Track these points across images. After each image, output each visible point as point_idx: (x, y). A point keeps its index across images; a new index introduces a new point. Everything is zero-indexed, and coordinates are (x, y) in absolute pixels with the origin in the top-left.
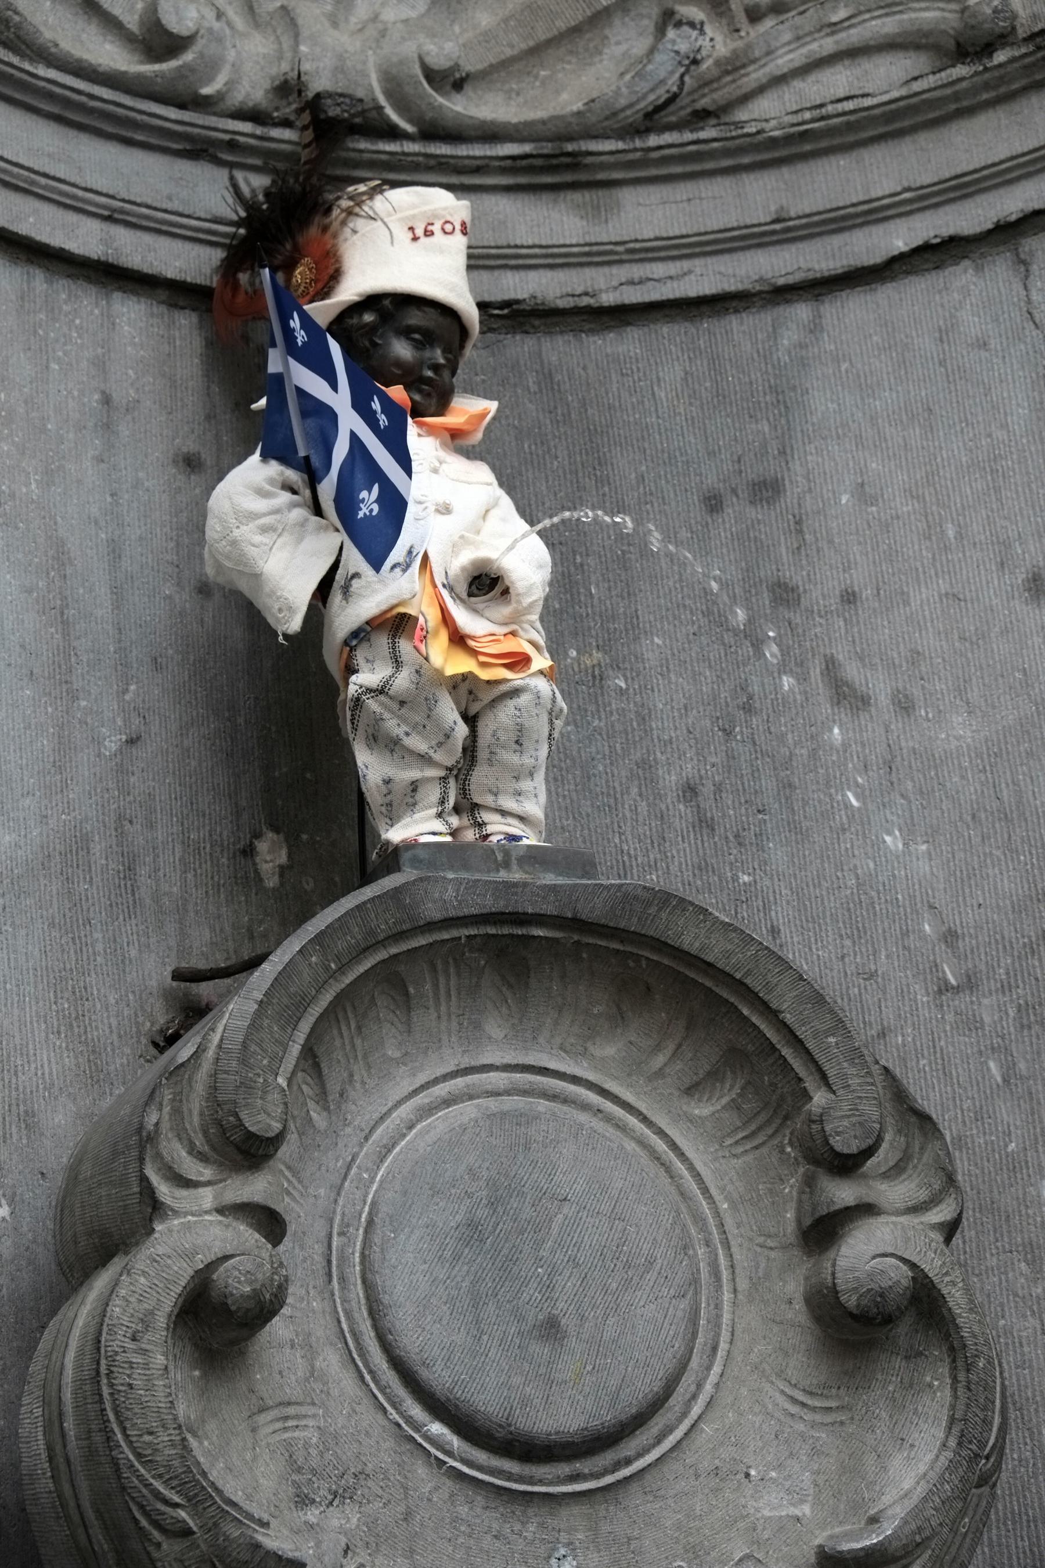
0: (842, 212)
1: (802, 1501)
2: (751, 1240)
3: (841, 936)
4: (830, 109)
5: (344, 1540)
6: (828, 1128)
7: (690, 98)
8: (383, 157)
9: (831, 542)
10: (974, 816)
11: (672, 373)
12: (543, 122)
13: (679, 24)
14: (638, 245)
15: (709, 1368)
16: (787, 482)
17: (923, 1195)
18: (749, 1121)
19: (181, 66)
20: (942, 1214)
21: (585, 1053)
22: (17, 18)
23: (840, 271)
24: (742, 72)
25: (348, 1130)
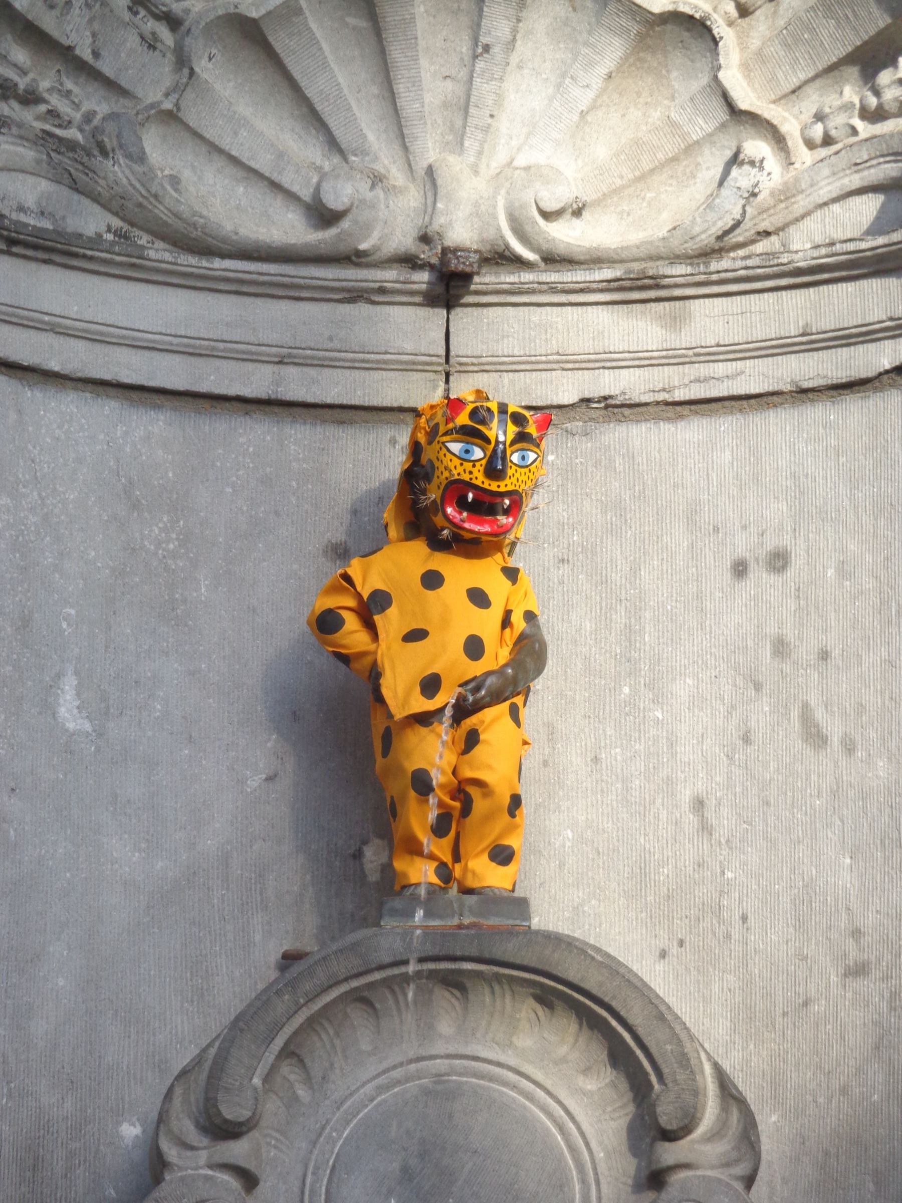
0: (847, 332)
2: (616, 1179)
3: (788, 924)
4: (838, 248)
7: (753, 222)
16: (793, 555)
17: (734, 1155)
19: (340, 233)
22: (202, 221)
23: (844, 381)
24: (793, 200)
25: (327, 1102)
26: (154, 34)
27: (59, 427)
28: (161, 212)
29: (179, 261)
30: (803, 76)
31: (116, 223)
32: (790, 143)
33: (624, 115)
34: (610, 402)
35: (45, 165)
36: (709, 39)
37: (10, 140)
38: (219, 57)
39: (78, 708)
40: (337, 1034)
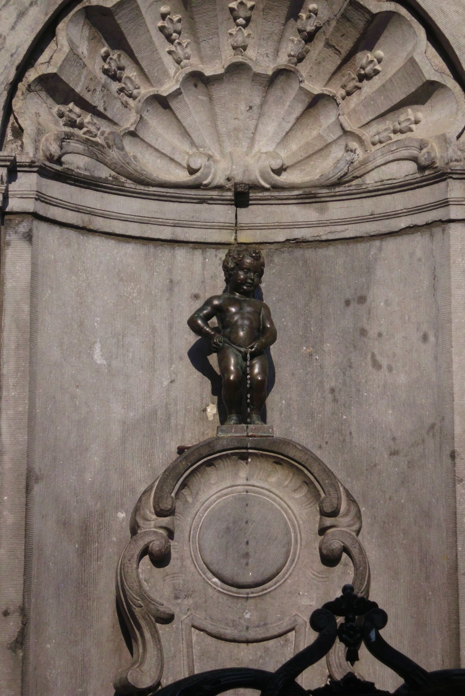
0: (388, 214)
1: (313, 601)
2: (307, 532)
5: (188, 607)
6: (324, 505)
8: (258, 197)
9: (377, 317)
10: (403, 405)
11: (340, 261)
12: (308, 182)
13: (347, 151)
14: (333, 221)
15: (291, 566)
17: (352, 522)
18: (308, 501)
20: (355, 527)
21: (266, 480)
22: (145, 172)
24: (367, 164)
25: (198, 503)
26: (126, 101)
27: (93, 250)
28: (130, 169)
29: (137, 188)
30: (371, 118)
31: (113, 173)
32: (366, 143)
33: (302, 133)
34: (297, 240)
35: (87, 151)
36: (335, 104)
37: (74, 141)
38: (151, 110)
39: (101, 355)
40: (202, 477)
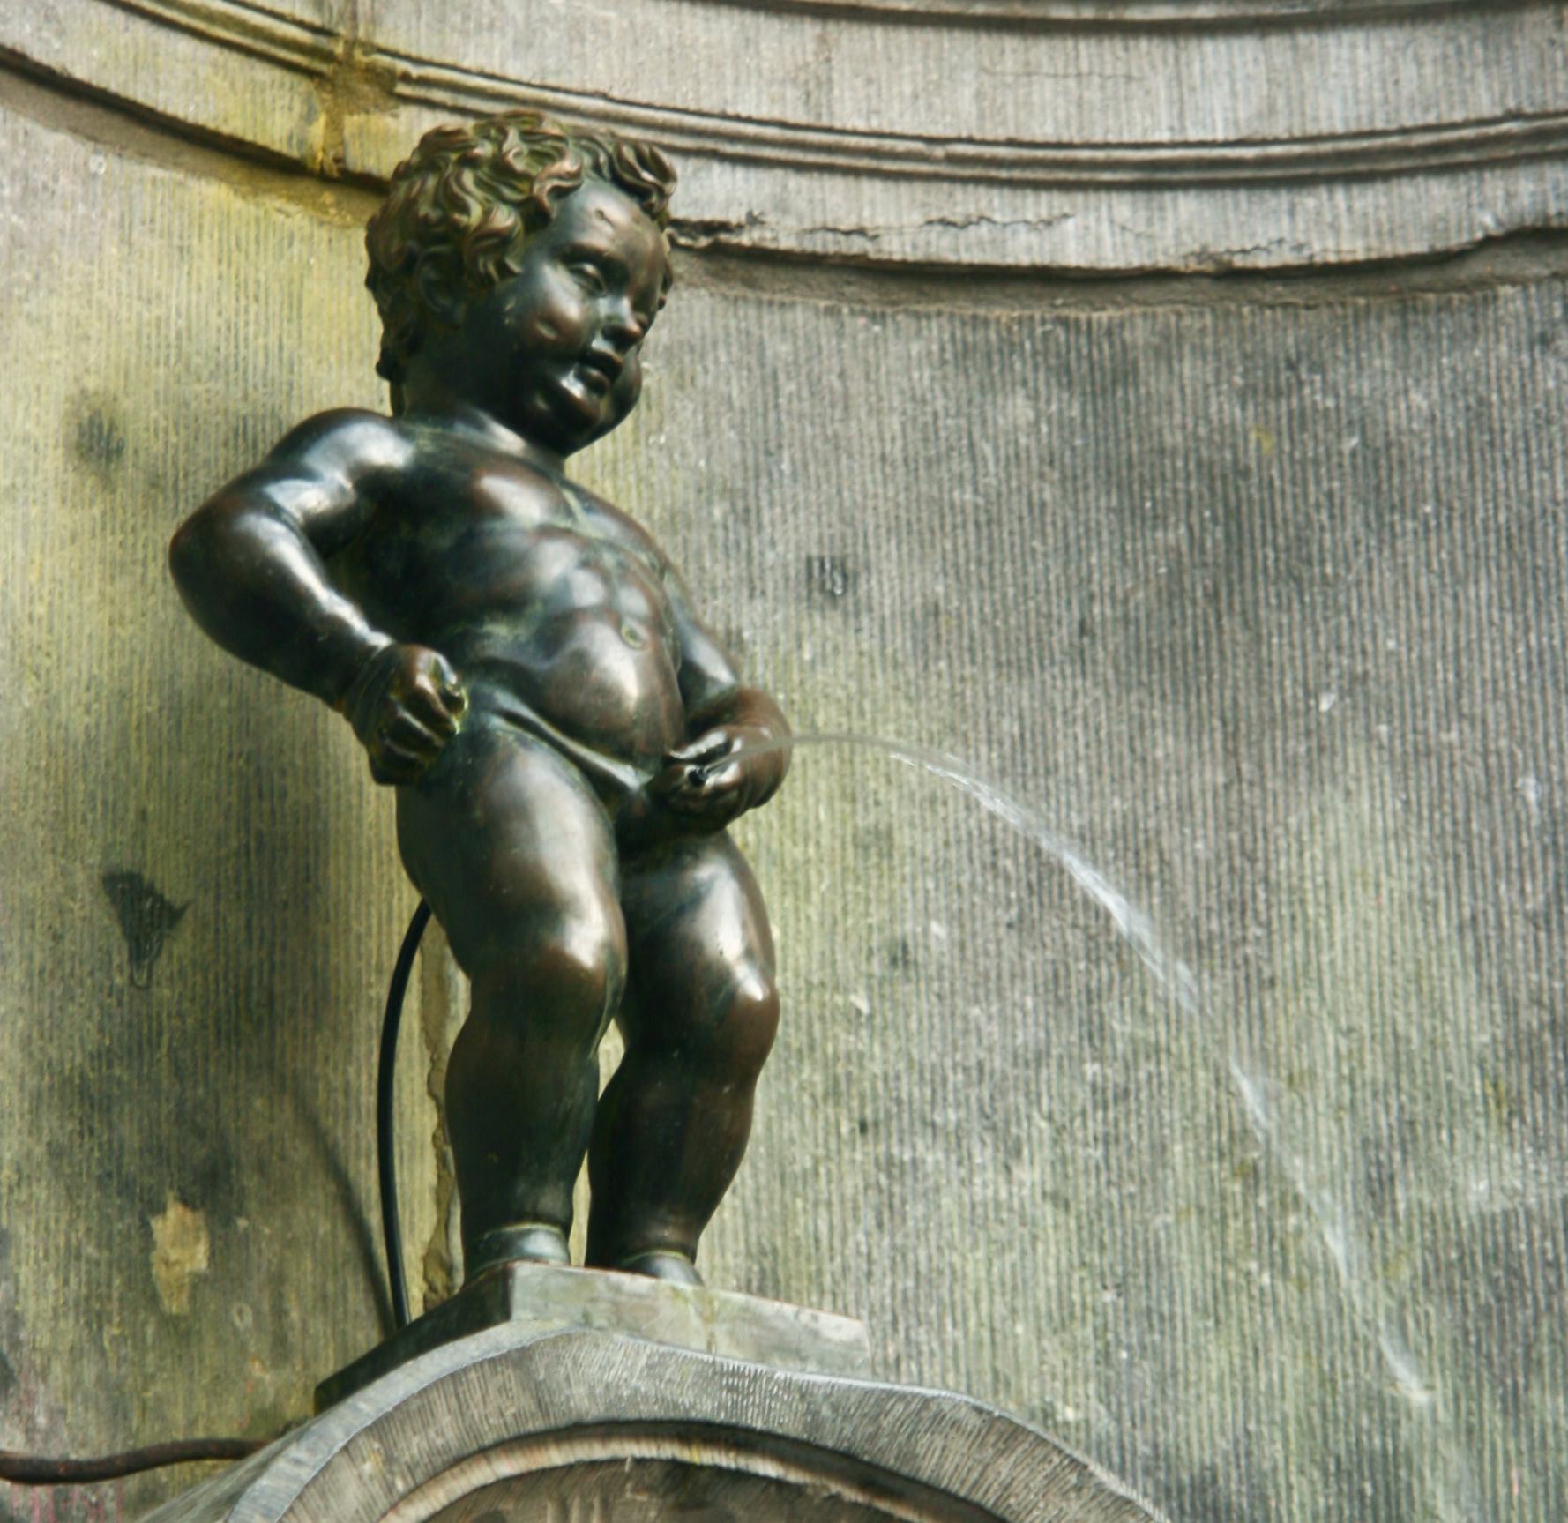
0: (1378, 142)
14: (970, 150)
34: (723, 237)
